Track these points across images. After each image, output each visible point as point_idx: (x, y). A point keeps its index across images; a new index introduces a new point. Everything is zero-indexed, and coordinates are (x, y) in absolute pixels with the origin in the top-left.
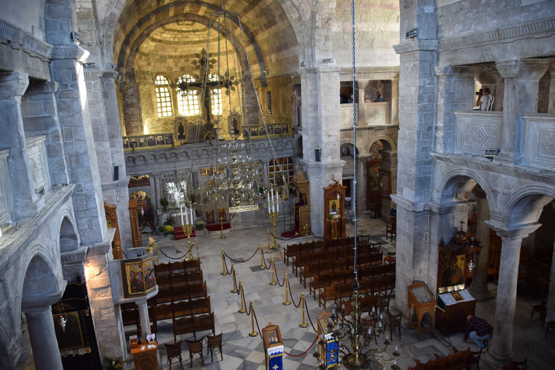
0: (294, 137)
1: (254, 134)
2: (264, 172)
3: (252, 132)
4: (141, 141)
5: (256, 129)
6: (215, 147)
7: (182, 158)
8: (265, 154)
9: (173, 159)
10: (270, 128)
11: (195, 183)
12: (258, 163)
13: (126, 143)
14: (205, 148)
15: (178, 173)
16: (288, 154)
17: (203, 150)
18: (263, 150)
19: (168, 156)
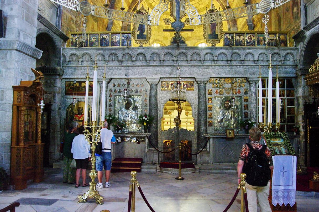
0: (297, 49)
1: (239, 43)
2: (251, 95)
3: (236, 41)
4: (93, 40)
5: (242, 38)
6: (183, 51)
7: (139, 63)
8: (253, 71)
9: (125, 64)
10: (262, 38)
11: (153, 99)
12: (242, 82)
13: (74, 41)
14: (170, 51)
15: (131, 83)
16: (286, 73)
17: (166, 54)
18: (250, 63)
19: (120, 58)
